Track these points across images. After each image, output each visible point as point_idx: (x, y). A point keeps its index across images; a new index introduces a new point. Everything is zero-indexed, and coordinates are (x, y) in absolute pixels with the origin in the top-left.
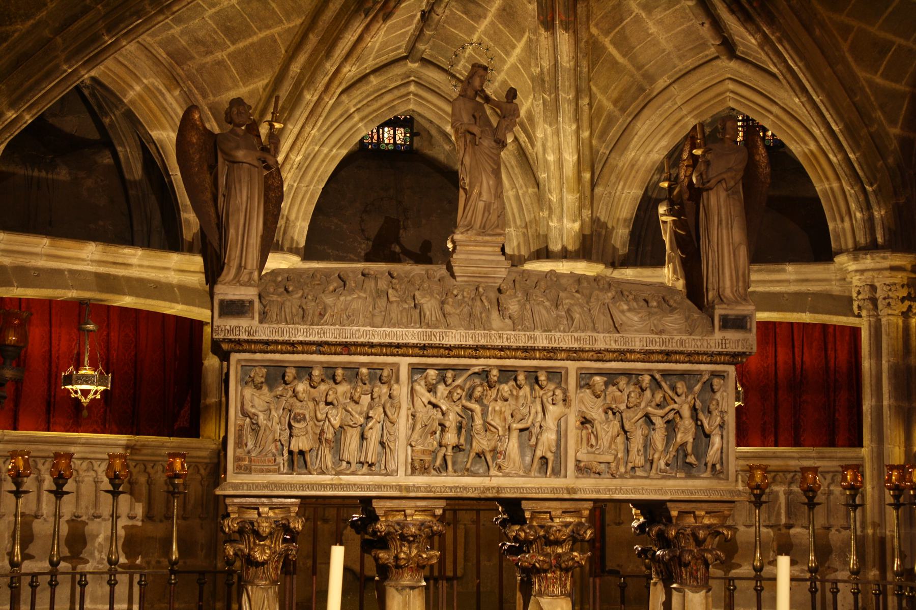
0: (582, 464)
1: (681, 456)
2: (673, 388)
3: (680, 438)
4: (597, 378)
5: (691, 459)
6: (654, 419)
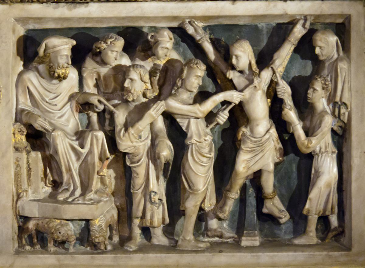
0: (31, 225)
1: (252, 200)
2: (226, 54)
3: (244, 165)
4: (54, 42)
5: (275, 206)
6: (183, 123)
